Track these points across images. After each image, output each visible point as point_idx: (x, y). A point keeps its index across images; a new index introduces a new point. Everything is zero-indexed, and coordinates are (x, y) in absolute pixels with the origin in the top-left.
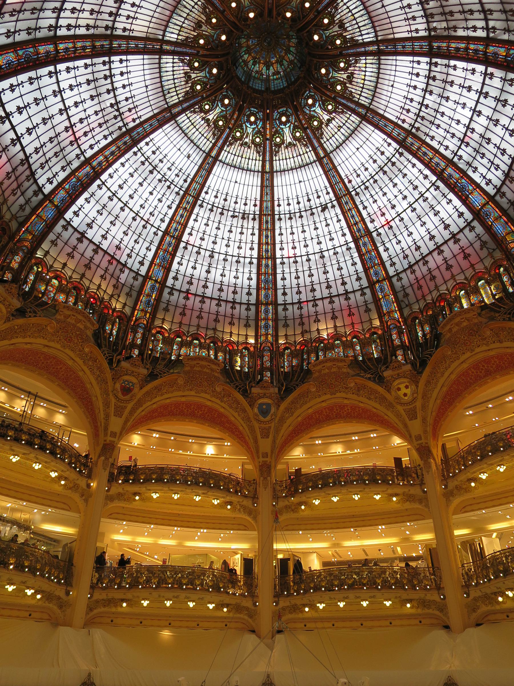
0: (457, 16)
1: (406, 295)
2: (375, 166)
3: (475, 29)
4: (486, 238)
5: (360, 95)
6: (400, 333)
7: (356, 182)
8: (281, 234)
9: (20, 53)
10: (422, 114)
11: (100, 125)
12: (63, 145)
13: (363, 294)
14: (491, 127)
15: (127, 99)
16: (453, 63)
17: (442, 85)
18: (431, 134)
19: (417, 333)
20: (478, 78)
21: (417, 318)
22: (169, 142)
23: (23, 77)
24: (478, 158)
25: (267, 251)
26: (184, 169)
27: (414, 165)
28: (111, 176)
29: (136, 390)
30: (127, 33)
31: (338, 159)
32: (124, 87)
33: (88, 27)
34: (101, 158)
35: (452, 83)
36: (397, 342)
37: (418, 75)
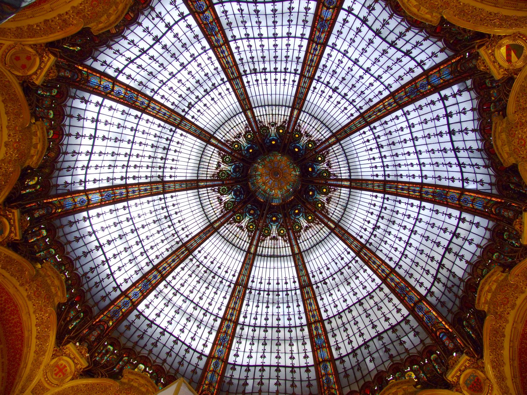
1: (230, 383)
2: (276, 286)
4: (314, 383)
7: (255, 285)
8: (183, 269)
9: (214, 23)
13: (200, 358)
16: (366, 267)
17: (351, 275)
18: (323, 296)
23: (197, 30)
24: (342, 329)
25: (165, 268)
27: (298, 306)
28: (148, 121)
30: (246, 84)
31: (259, 263)
32: (213, 99)
33: (241, 59)
34: (158, 108)
35: (357, 278)
37: (342, 259)
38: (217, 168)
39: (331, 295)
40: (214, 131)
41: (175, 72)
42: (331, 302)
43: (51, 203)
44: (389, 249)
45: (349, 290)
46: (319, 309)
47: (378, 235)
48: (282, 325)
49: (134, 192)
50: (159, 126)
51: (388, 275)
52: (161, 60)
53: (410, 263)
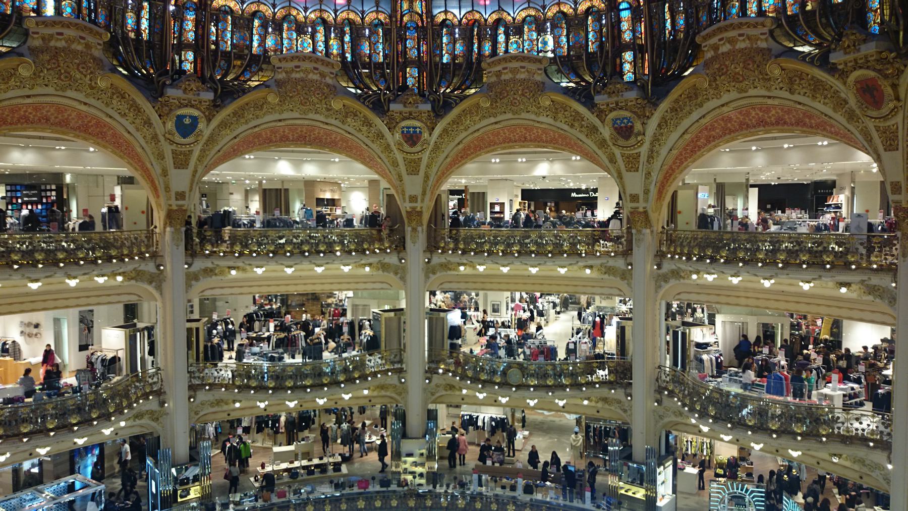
29: (201, 126)
36: (627, 36)
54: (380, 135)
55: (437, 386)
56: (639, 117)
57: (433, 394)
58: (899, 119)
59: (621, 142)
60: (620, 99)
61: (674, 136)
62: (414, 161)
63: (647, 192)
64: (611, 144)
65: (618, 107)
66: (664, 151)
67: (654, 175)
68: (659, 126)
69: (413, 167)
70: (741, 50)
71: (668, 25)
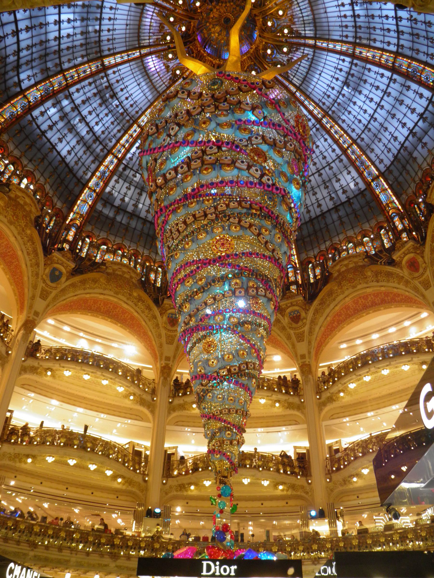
0: (378, 32)
3: (389, 43)
5: (294, 77)
6: (295, 274)
10: (339, 101)
11: (82, 45)
12: (48, 51)
14: (389, 118)
15: (109, 30)
18: (343, 117)
19: (309, 276)
20: (385, 80)
21: (310, 262)
22: (132, 76)
26: (139, 102)
29: (63, 279)
38: (168, 72)
39: (350, 112)
40: (136, 43)
41: (56, 34)
42: (353, 119)
43: (71, 220)
44: (382, 33)
45: (363, 99)
46: (346, 132)
47: (362, 24)
48: (321, 167)
49: (119, 151)
50: (90, 84)
51: (393, 63)
52: (36, 40)
53: (410, 38)
54: (155, 317)
55: (171, 487)
56: (303, 309)
57: (166, 494)
58: (428, 273)
59: (294, 325)
60: (293, 300)
61: (322, 319)
62: (171, 336)
63: (309, 353)
64: (287, 328)
65: (292, 305)
66: (317, 329)
67: (313, 343)
68: (314, 314)
69: (170, 342)
70: (351, 268)
71: (311, 276)
